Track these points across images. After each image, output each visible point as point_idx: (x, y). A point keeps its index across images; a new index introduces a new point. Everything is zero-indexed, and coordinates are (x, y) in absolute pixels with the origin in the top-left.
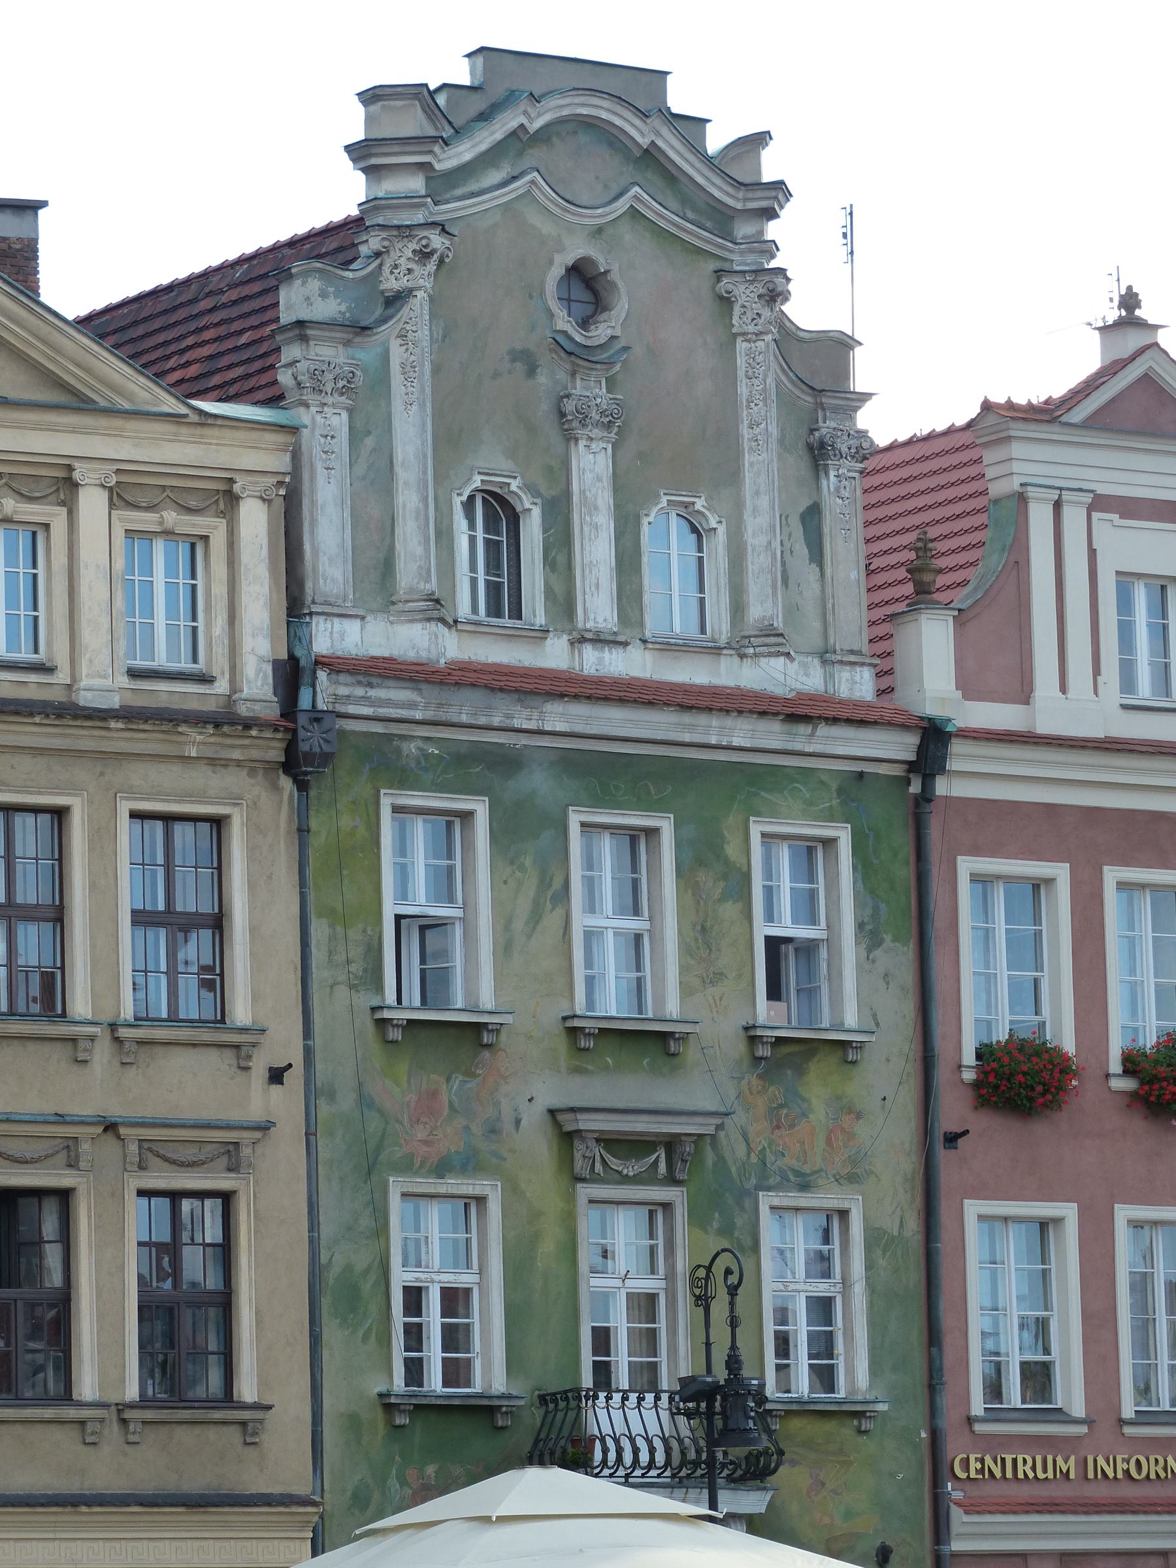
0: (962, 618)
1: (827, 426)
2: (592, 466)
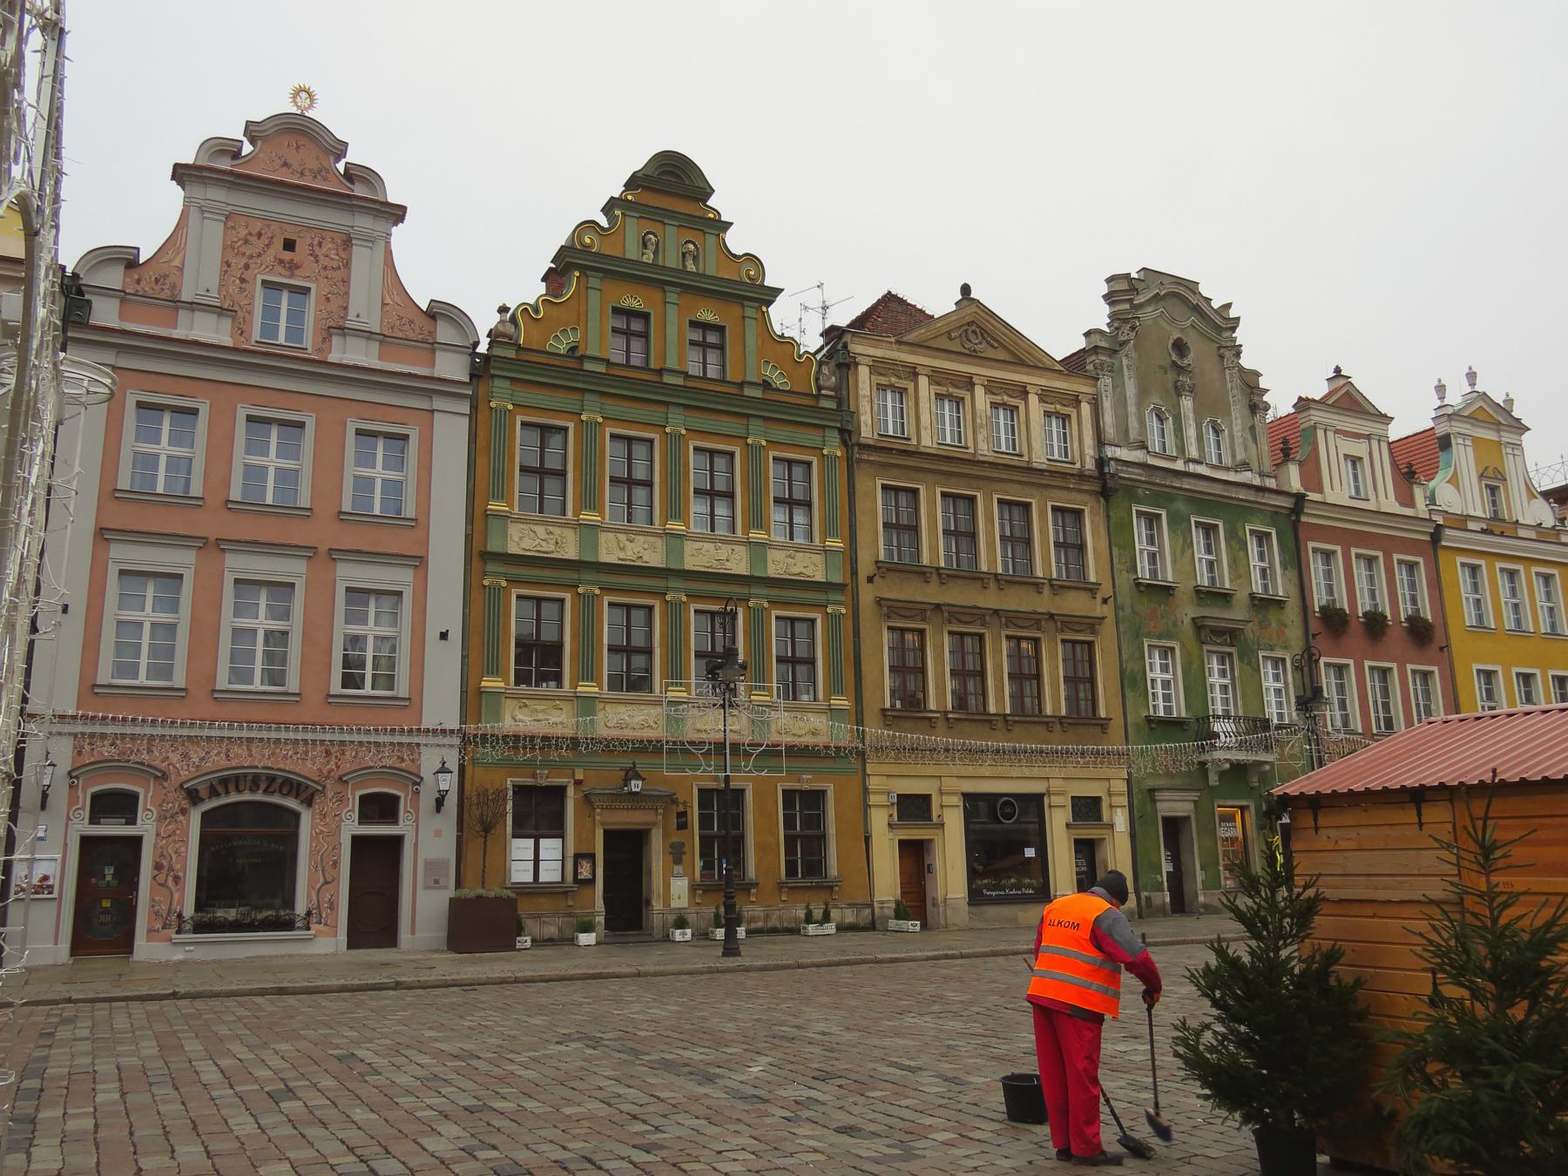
0: (1301, 464)
1: (1256, 399)
2: (1187, 404)
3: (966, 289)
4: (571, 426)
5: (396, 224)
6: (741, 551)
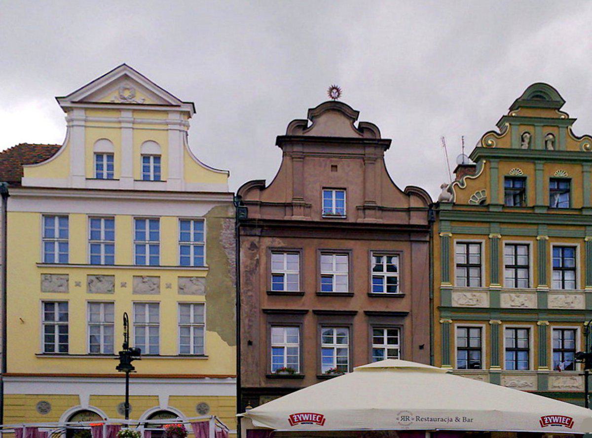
4: (484, 241)
5: (385, 150)
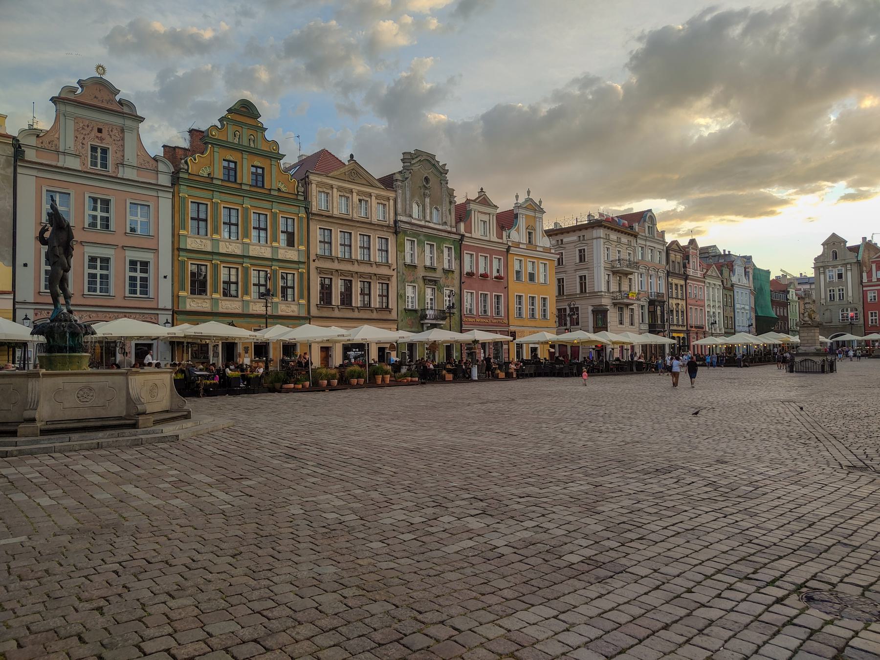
2: (427, 200)
3: (352, 156)
6: (269, 249)
